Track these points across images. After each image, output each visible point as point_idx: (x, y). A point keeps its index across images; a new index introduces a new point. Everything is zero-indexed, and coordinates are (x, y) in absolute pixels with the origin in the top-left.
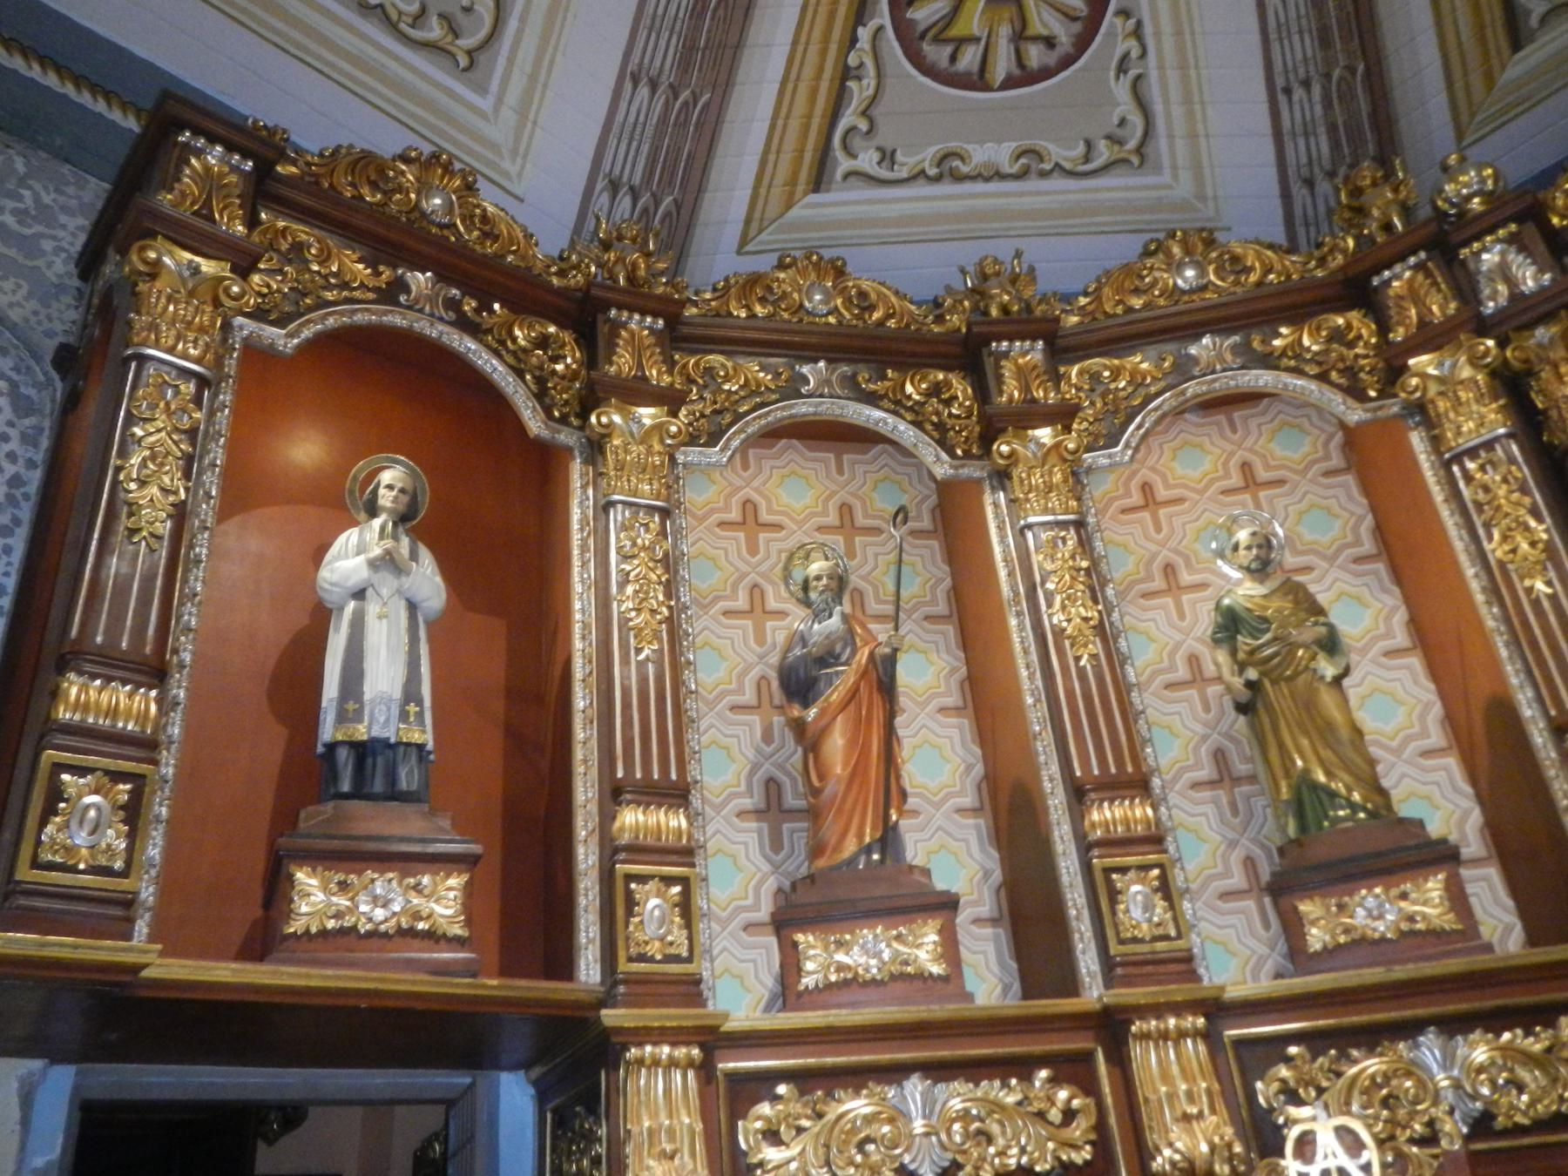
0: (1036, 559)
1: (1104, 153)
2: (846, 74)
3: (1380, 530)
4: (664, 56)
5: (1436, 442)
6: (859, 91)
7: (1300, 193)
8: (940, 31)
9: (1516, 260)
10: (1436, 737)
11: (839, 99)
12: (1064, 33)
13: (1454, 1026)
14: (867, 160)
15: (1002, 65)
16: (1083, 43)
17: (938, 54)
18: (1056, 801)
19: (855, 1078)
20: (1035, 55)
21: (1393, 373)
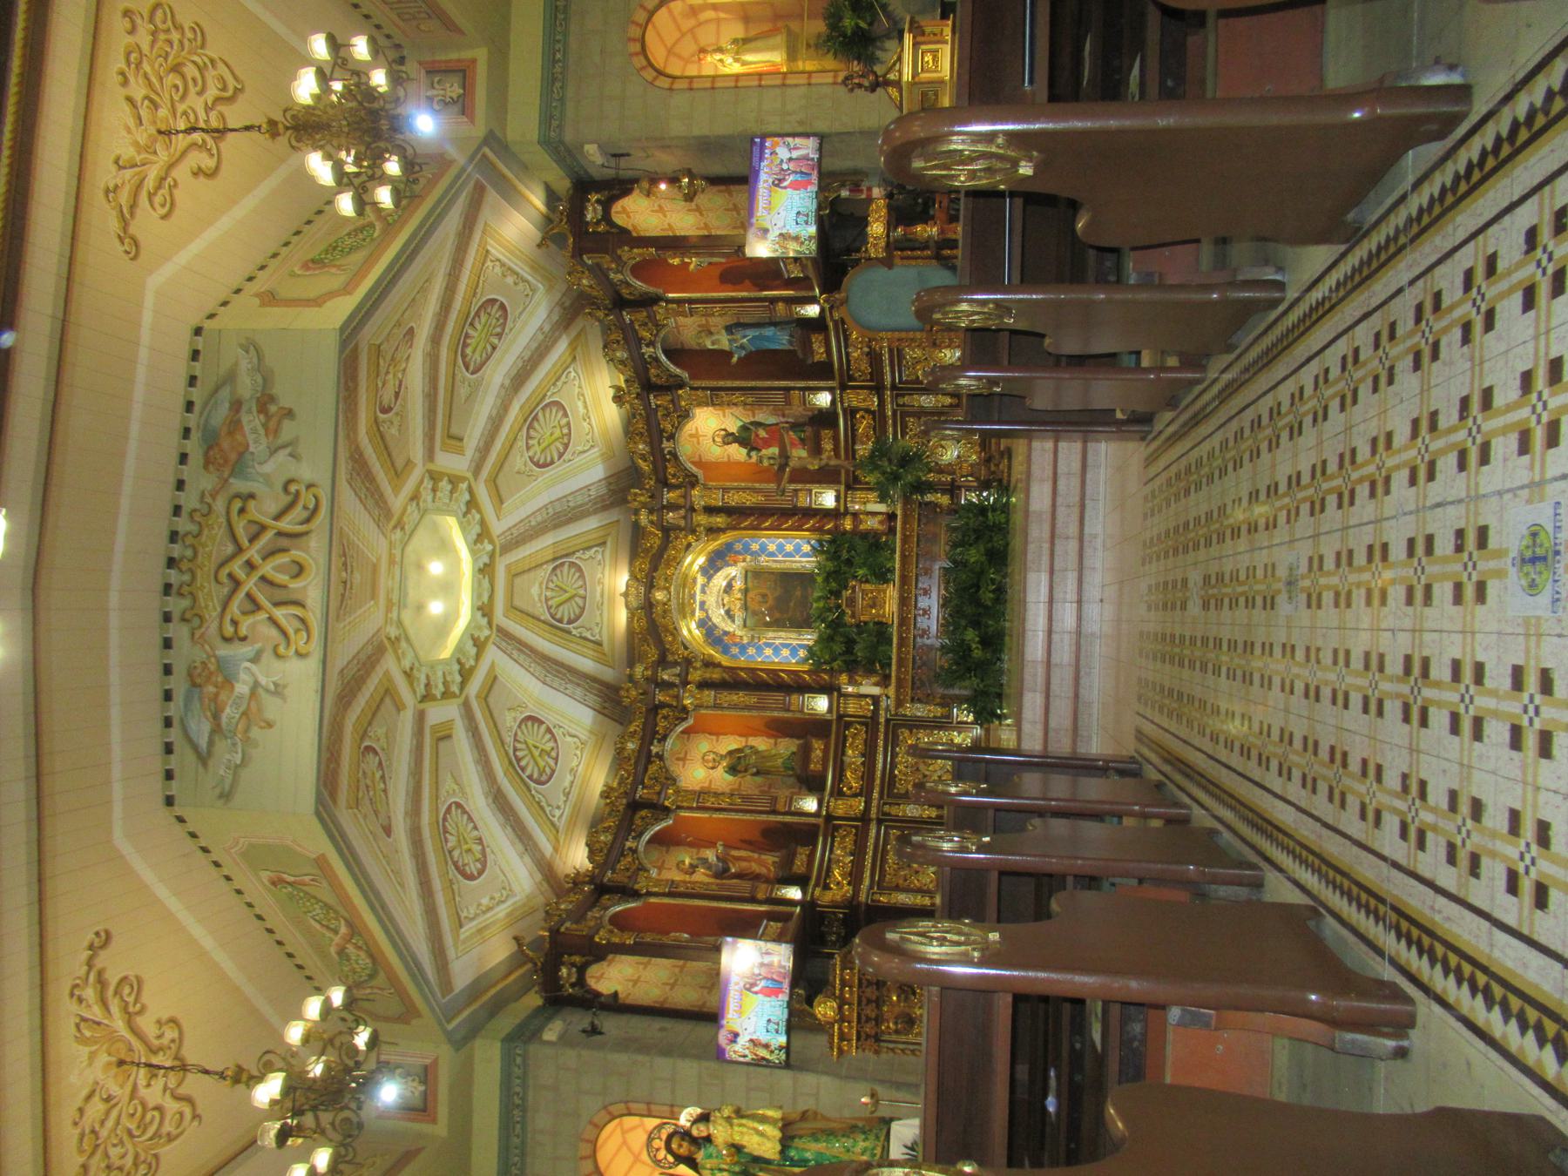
0: (708, 804)
1: (578, 752)
2: (538, 803)
3: (710, 734)
4: (520, 847)
5: (707, 707)
6: (544, 804)
7: (606, 711)
8: (541, 774)
9: (669, 671)
10: (772, 741)
11: (542, 808)
12: (551, 744)
13: (843, 753)
14: (557, 813)
15: (552, 762)
16: (556, 741)
17: (544, 778)
18: (772, 818)
19: (829, 870)
20: (554, 754)
21: (684, 709)
